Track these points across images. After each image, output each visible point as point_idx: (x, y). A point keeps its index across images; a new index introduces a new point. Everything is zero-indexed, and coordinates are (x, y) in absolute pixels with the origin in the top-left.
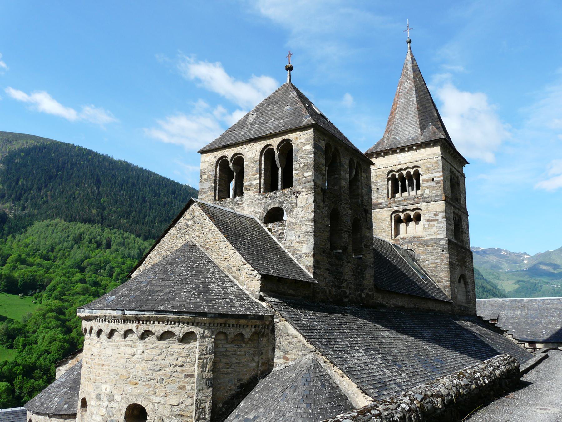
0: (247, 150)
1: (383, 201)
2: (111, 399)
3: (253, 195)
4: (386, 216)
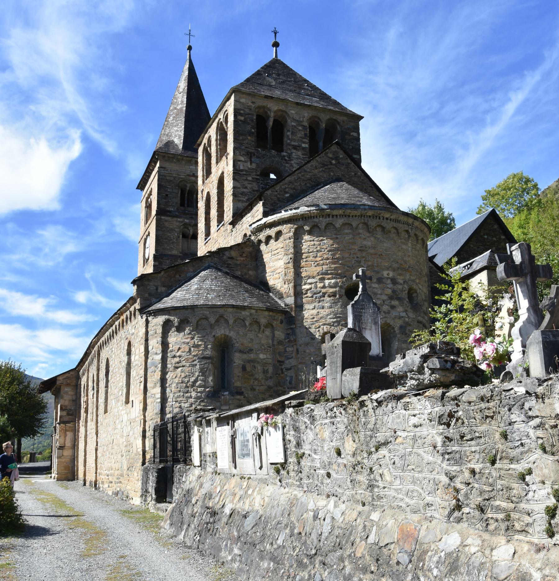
0: (293, 112)
1: (172, 209)
2: (394, 281)
3: (301, 156)
4: (175, 226)
